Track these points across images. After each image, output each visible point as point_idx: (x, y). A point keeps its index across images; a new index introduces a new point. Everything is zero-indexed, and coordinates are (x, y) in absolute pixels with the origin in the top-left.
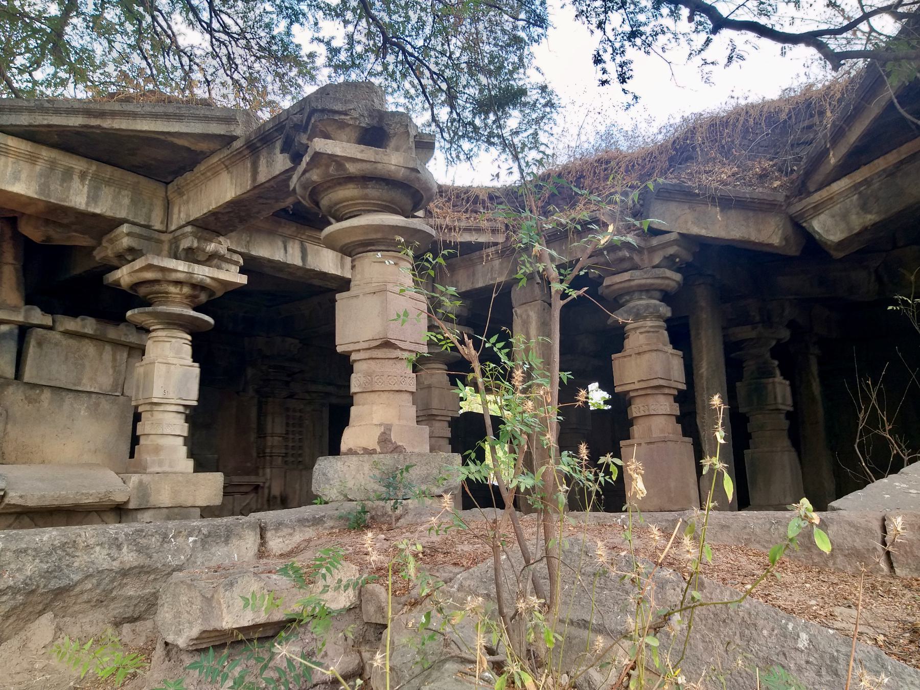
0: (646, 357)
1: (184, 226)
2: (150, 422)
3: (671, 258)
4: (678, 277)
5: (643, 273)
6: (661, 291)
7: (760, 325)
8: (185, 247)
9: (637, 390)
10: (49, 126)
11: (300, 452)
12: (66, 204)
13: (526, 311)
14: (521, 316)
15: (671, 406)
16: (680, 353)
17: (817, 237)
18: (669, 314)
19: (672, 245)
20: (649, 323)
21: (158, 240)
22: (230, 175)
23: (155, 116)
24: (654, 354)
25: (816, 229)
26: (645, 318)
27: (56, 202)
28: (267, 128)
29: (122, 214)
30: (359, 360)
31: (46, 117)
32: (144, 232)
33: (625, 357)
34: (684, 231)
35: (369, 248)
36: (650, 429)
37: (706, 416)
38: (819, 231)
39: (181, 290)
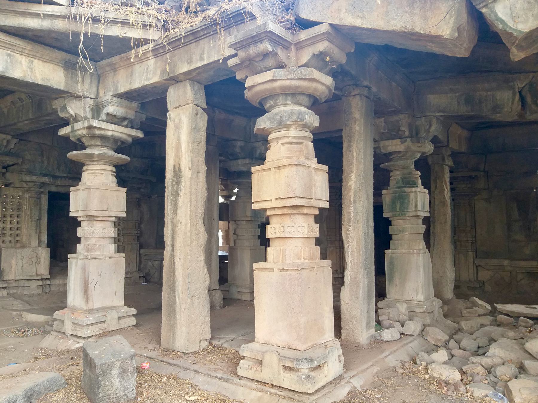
0: (285, 171)
3: (320, 56)
4: (329, 81)
5: (287, 73)
6: (310, 96)
7: (408, 140)
11: (18, 232)
13: (179, 115)
14: (174, 121)
15: (309, 227)
16: (326, 168)
17: (500, 26)
18: (317, 124)
19: (322, 40)
20: (292, 133)
24: (294, 169)
25: (500, 15)
26: (288, 127)
33: (264, 170)
34: (336, 22)
36: (284, 254)
37: (351, 228)
38: (504, 18)
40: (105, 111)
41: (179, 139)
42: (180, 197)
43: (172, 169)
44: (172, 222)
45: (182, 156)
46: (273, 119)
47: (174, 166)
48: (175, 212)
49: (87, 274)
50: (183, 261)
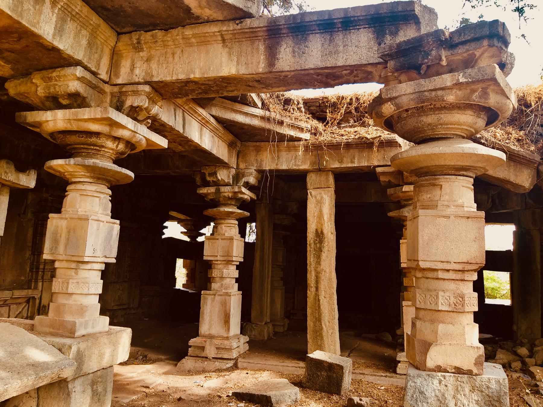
1: (139, 83)
2: (75, 281)
8: (136, 104)
12: (36, 30)
13: (321, 194)
14: (316, 197)
21: (102, 90)
22: (227, 50)
27: (27, 25)
28: (307, 19)
29: (79, 55)
30: (444, 279)
32: (94, 80)
35: (461, 173)
39: (117, 146)
40: (244, 180)
41: (321, 211)
42: (323, 253)
43: (314, 231)
44: (315, 270)
45: (324, 223)
47: (317, 230)
48: (318, 263)
49: (228, 308)
50: (328, 299)
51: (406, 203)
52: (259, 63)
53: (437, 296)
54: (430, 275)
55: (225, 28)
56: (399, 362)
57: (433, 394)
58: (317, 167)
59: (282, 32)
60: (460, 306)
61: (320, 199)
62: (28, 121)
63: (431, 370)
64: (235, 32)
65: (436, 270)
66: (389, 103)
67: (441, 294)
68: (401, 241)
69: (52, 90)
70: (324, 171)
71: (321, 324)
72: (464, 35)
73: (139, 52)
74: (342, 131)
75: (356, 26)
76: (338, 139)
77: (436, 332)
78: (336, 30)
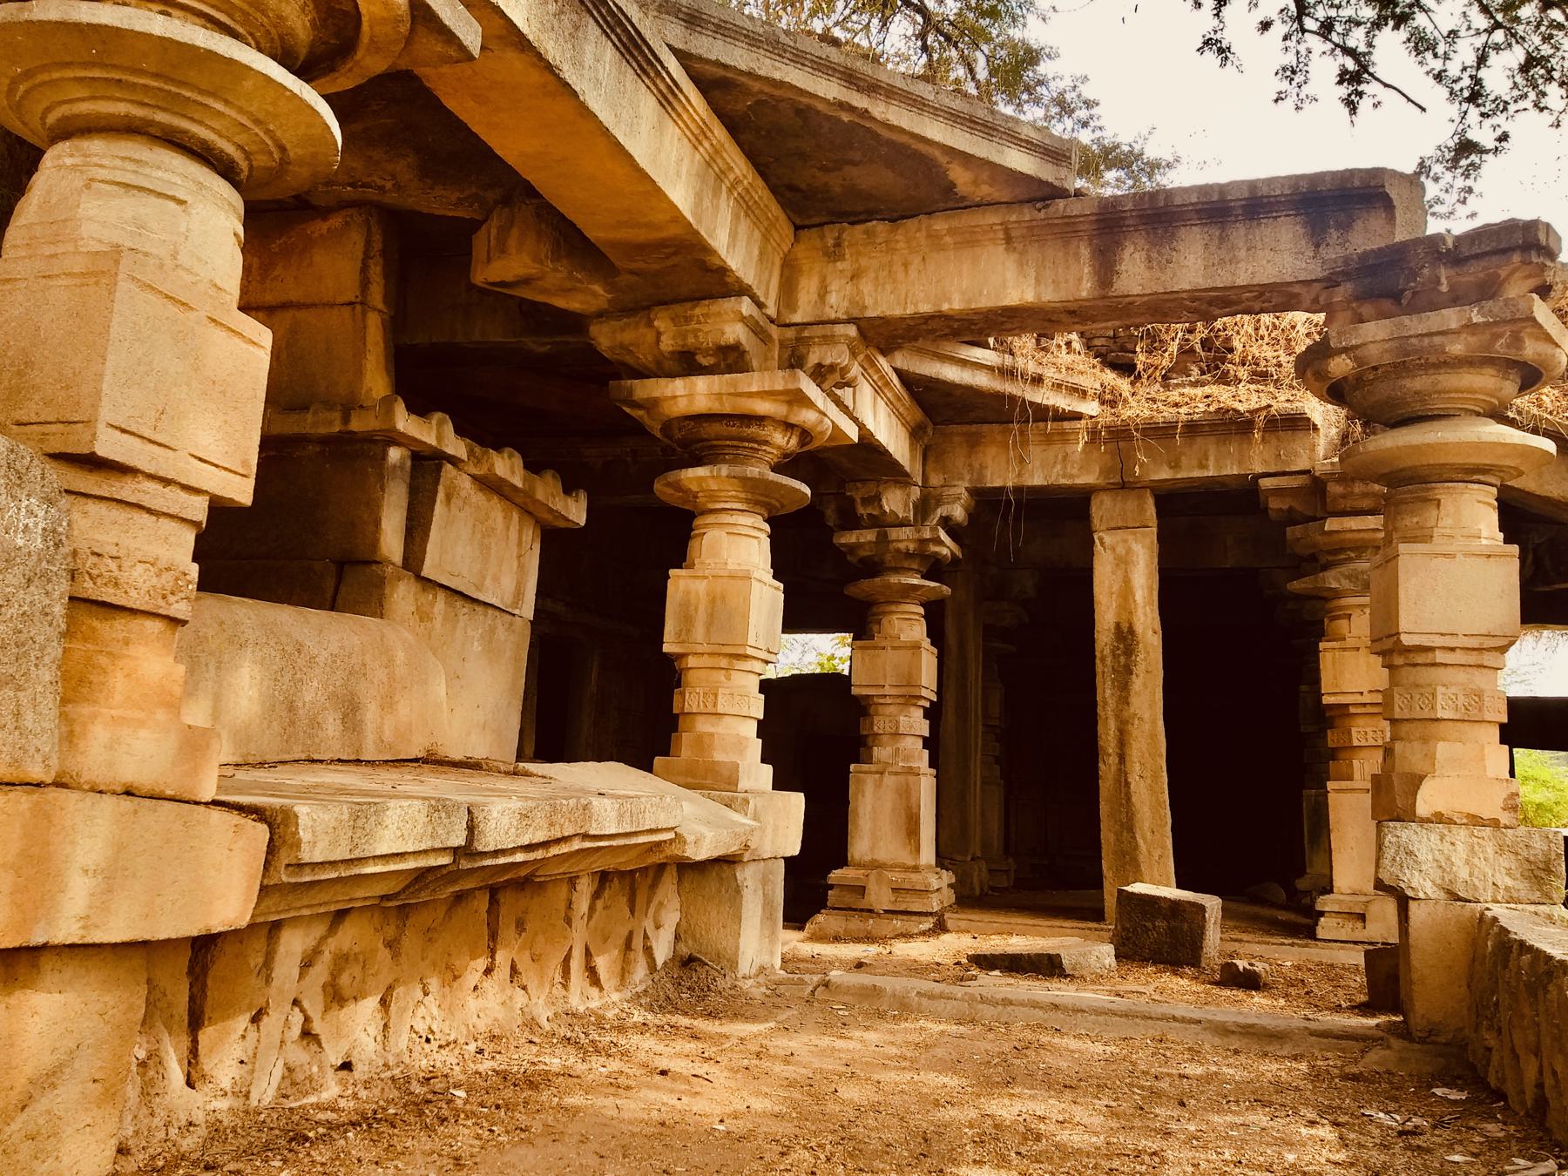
8: (828, 362)
9: (1364, 705)
10: (781, 84)
13: (1125, 541)
14: (1113, 549)
22: (1015, 256)
23: (954, 118)
28: (1178, 201)
30: (1446, 665)
31: (777, 64)
33: (1344, 649)
35: (1475, 477)
39: (788, 441)
40: (941, 511)
41: (1127, 581)
44: (1117, 717)
46: (1357, 579)
47: (1118, 625)
48: (1124, 700)
49: (913, 800)
50: (1149, 781)
51: (1331, 558)
52: (1080, 280)
53: (1434, 695)
54: (1420, 659)
55: (1014, 218)
56: (1322, 914)
57: (1430, 857)
58: (1117, 479)
59: (1127, 223)
60: (1476, 711)
61: (1124, 552)
62: (635, 398)
63: (1424, 821)
64: (1034, 223)
65: (1431, 649)
66: (1344, 356)
67: (1440, 690)
68: (1322, 645)
69: (691, 340)
70: (1134, 489)
71: (1134, 838)
72: (1480, 244)
73: (835, 261)
74: (1174, 396)
75: (1271, 212)
76: (1168, 413)
77: (1431, 757)
78: (1233, 219)
